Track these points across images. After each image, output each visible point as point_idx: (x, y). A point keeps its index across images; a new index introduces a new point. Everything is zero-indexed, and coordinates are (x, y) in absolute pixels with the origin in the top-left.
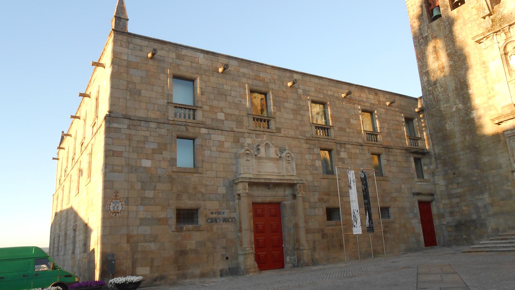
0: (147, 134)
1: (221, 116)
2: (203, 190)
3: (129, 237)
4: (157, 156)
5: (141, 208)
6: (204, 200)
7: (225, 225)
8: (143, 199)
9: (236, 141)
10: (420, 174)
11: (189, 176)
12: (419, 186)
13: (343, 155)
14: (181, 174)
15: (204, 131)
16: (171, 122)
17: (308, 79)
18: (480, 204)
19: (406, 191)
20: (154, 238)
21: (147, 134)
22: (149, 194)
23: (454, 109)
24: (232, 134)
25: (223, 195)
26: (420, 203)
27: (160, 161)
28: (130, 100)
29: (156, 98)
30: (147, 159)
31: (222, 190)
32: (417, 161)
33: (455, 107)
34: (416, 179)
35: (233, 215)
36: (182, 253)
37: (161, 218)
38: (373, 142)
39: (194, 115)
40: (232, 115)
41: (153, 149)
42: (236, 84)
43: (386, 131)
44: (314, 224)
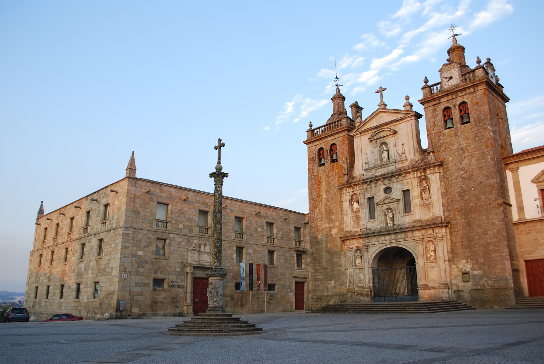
0: (142, 237)
1: (181, 226)
2: (168, 269)
3: (130, 292)
4: (146, 249)
5: (137, 277)
6: (168, 275)
7: (178, 289)
8: (138, 272)
9: (188, 241)
10: (299, 264)
11: (161, 261)
12: (297, 272)
13: (250, 251)
14: (157, 260)
15: (171, 235)
16: (155, 230)
17: (234, 202)
18: (329, 286)
19: (288, 275)
20: (142, 294)
21: (142, 237)
22: (141, 270)
23: (324, 226)
24: (186, 237)
25: (179, 272)
26: (296, 282)
27: (147, 252)
28: (134, 217)
29: (147, 216)
30: (141, 251)
31: (178, 270)
32: (299, 256)
33: (325, 225)
34: (296, 268)
35: (182, 284)
36: (155, 302)
37: (146, 283)
38: (271, 243)
39: (166, 226)
40: (187, 225)
41: (144, 245)
42: (192, 207)
43: (280, 236)
44: (228, 292)
